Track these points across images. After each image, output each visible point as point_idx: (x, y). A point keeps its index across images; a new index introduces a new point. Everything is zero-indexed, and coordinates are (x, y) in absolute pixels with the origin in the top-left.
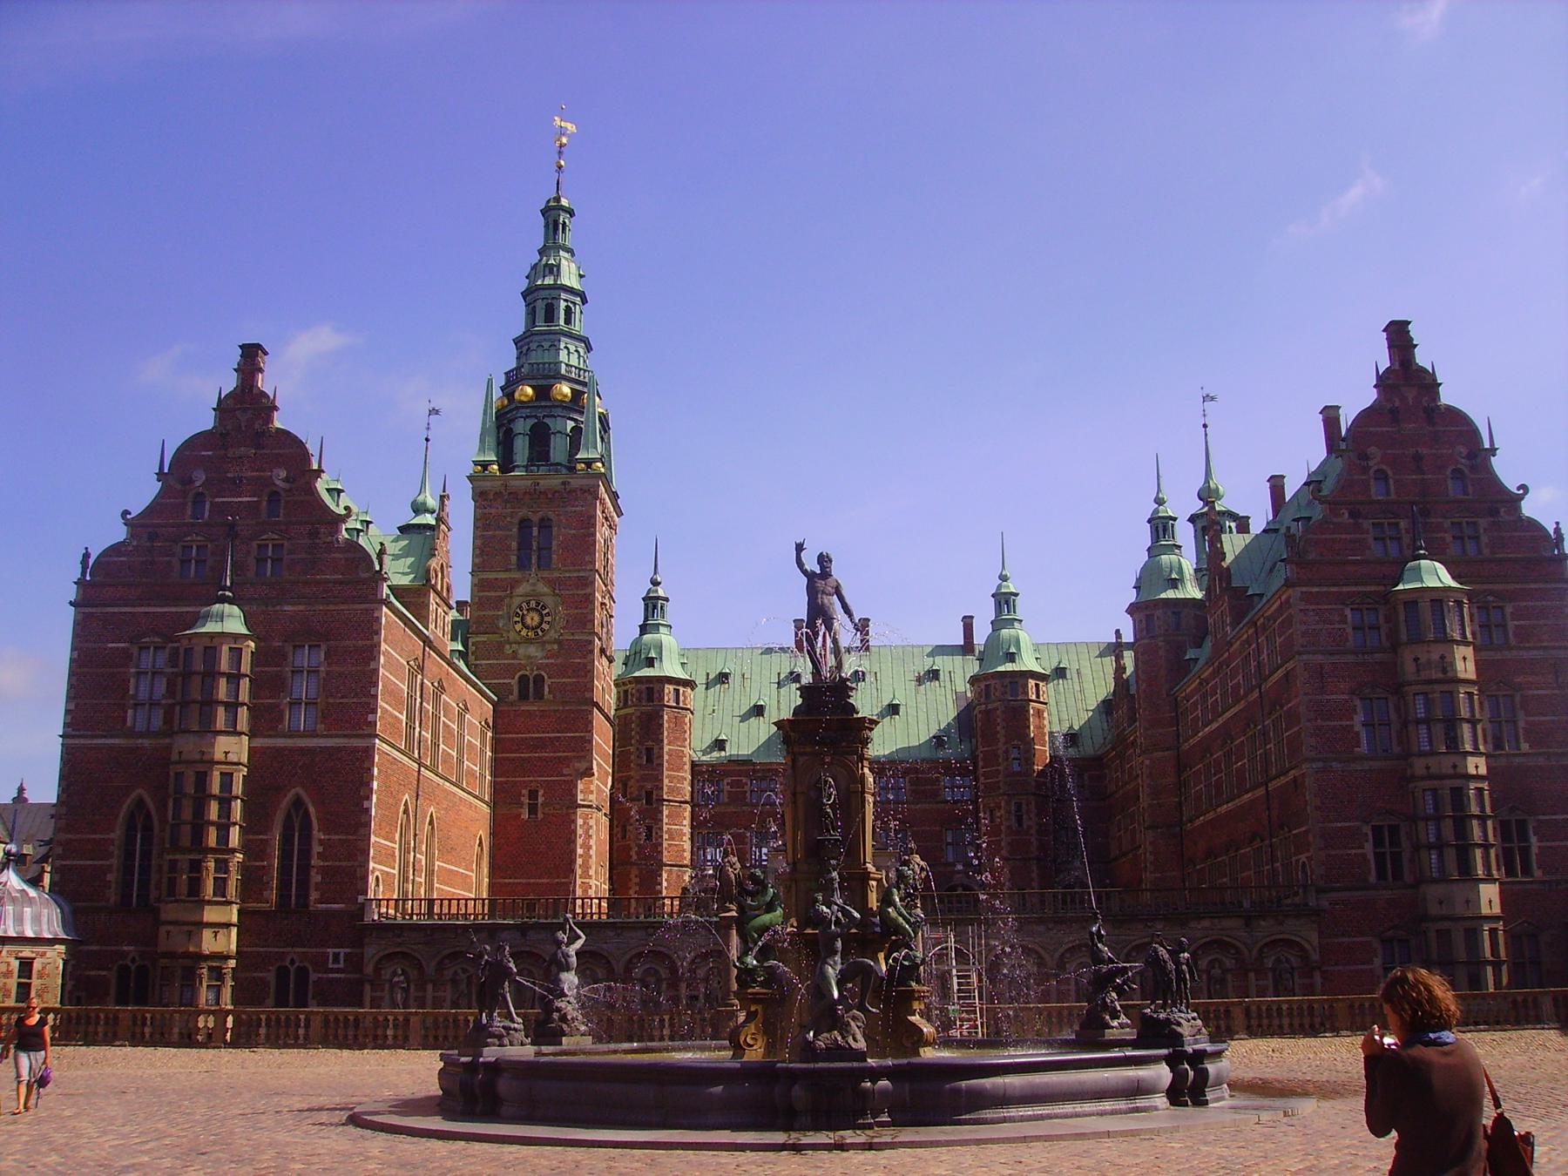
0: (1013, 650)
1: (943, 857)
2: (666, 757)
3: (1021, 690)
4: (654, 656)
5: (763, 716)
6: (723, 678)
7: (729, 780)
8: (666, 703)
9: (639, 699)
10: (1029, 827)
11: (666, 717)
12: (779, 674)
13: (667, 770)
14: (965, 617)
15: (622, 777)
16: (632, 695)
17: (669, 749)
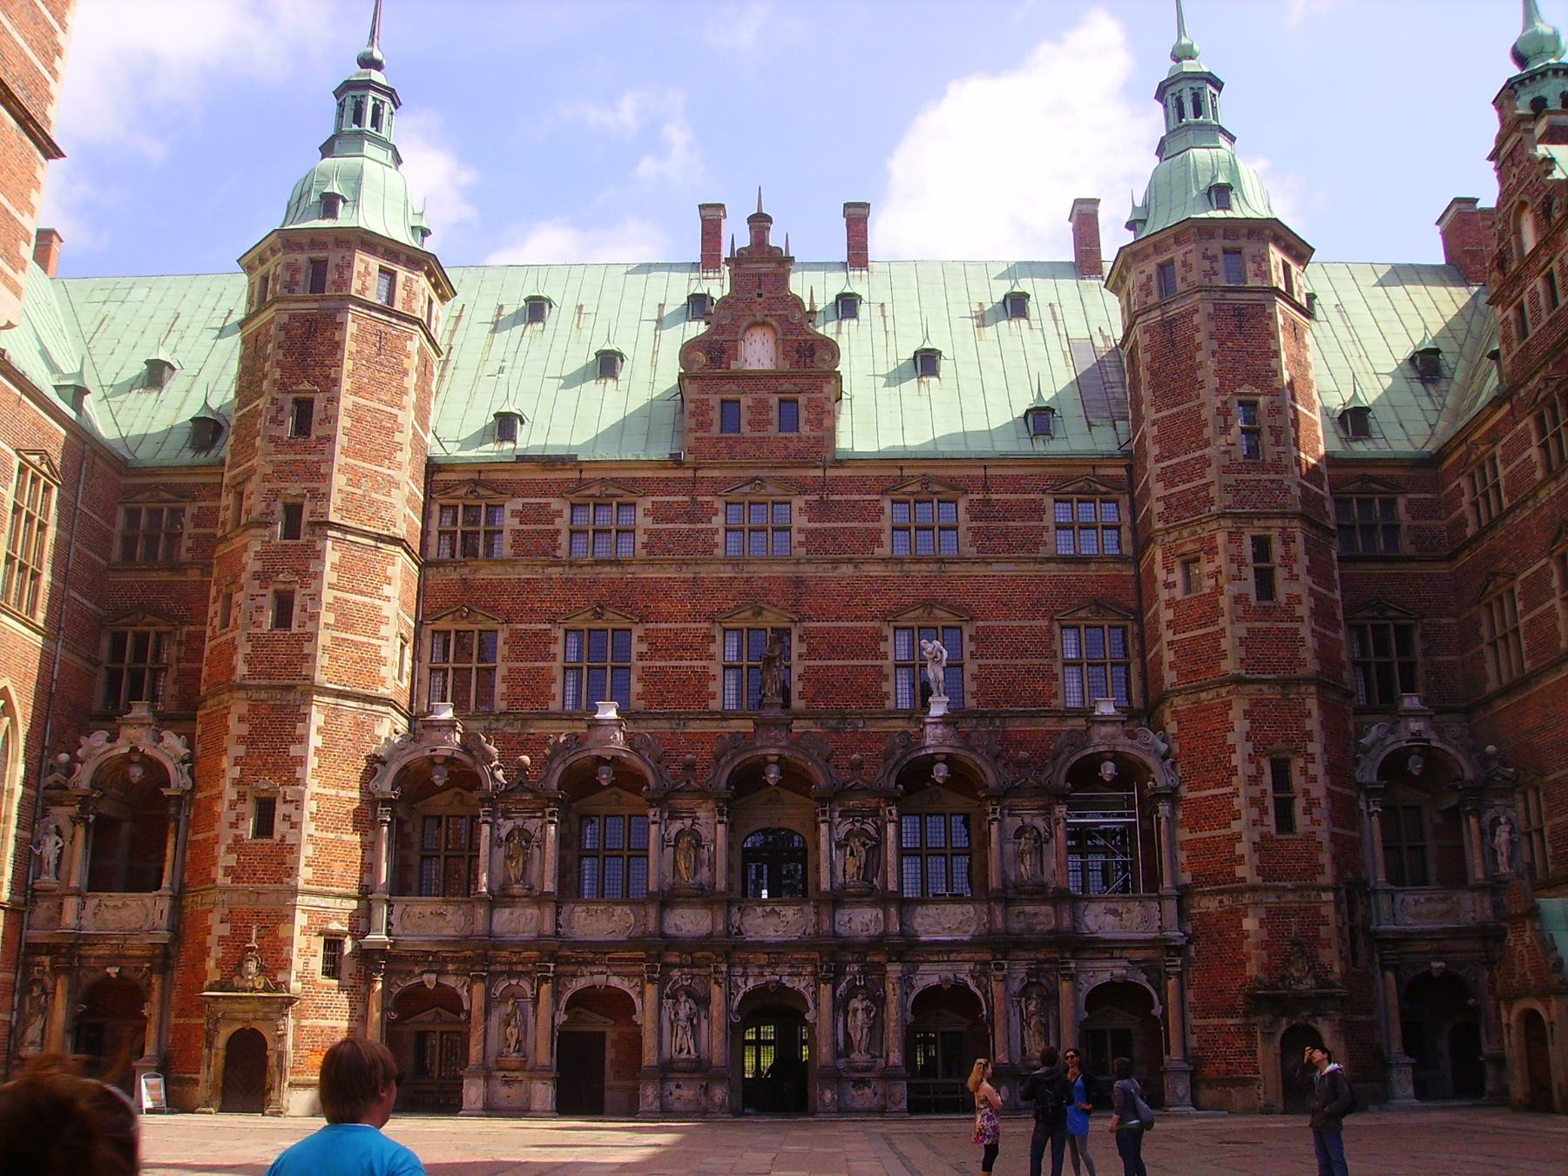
0: (1222, 180)
1: (1055, 695)
2: (344, 422)
3: (1251, 267)
4: (337, 191)
5: (614, 376)
6: (536, 309)
7: (517, 504)
8: (353, 293)
9: (290, 286)
10: (1294, 599)
11: (351, 328)
12: (661, 306)
13: (345, 452)
14: (1077, 202)
15: (235, 477)
16: (275, 279)
17: (355, 404)
